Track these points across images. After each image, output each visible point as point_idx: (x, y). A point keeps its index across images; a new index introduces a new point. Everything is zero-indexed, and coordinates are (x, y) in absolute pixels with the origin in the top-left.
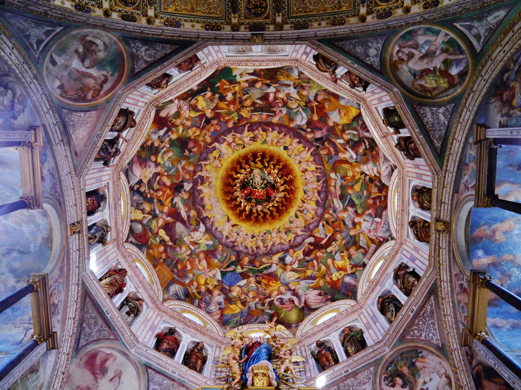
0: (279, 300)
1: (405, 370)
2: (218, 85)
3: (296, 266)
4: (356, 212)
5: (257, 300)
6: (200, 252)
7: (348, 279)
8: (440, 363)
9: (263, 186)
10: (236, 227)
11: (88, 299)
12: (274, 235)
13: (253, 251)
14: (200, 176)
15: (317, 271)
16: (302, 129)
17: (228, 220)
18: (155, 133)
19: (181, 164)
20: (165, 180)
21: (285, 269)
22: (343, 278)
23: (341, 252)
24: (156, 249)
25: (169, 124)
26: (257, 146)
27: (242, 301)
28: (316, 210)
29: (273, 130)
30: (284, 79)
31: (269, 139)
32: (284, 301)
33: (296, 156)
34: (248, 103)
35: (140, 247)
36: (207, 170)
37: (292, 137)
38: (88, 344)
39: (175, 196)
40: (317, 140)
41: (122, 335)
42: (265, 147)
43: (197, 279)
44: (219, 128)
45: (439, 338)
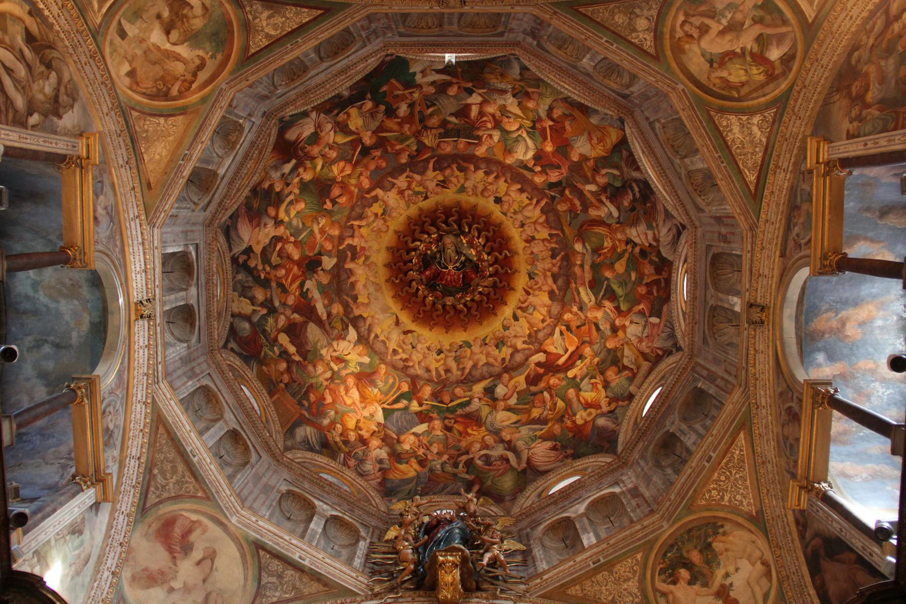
0: (484, 458)
1: (695, 557)
2: (385, 88)
3: (513, 401)
4: (617, 308)
5: (445, 457)
6: (347, 375)
7: (601, 422)
8: (754, 542)
9: (458, 265)
10: (410, 335)
11: (161, 430)
12: (476, 349)
13: (438, 375)
14: (348, 244)
15: (550, 410)
16: (526, 167)
17: (397, 323)
18: (276, 168)
19: (319, 223)
20: (290, 249)
21: (494, 408)
22: (594, 420)
23: (591, 378)
24: (273, 366)
25: (300, 153)
26: (449, 196)
27: (420, 458)
28: (549, 307)
29: (477, 168)
30: (495, 81)
31: (469, 184)
32: (492, 459)
33: (515, 213)
34: (434, 121)
35: (246, 359)
36: (362, 236)
37: (509, 180)
38: (160, 502)
39: (306, 279)
40: (551, 186)
42: (462, 197)
43: (342, 420)
44: (384, 164)
45: (752, 501)
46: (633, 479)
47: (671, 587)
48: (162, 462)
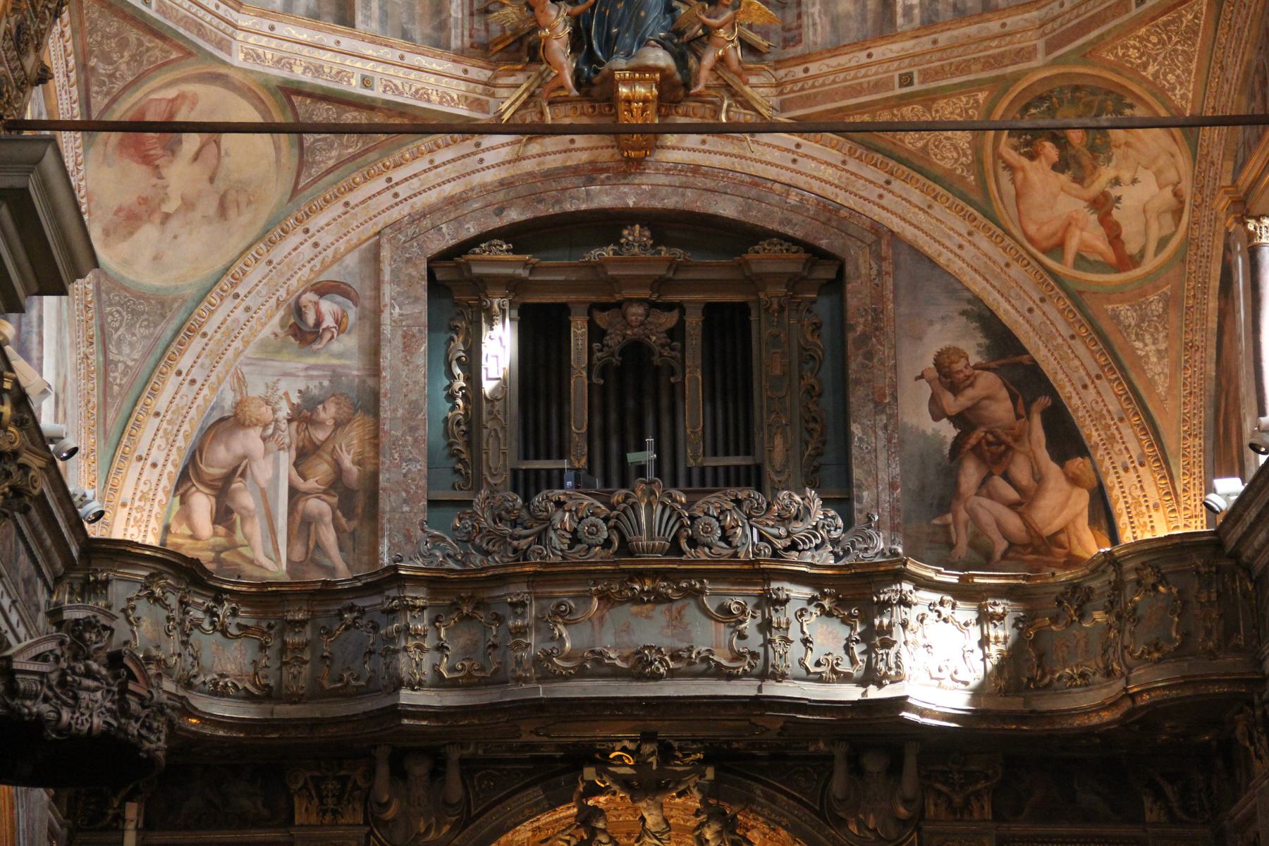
8: (1173, 156)
38: (114, 100)
41: (200, 29)
45: (1190, 95)
47: (1025, 162)
48: (100, 44)
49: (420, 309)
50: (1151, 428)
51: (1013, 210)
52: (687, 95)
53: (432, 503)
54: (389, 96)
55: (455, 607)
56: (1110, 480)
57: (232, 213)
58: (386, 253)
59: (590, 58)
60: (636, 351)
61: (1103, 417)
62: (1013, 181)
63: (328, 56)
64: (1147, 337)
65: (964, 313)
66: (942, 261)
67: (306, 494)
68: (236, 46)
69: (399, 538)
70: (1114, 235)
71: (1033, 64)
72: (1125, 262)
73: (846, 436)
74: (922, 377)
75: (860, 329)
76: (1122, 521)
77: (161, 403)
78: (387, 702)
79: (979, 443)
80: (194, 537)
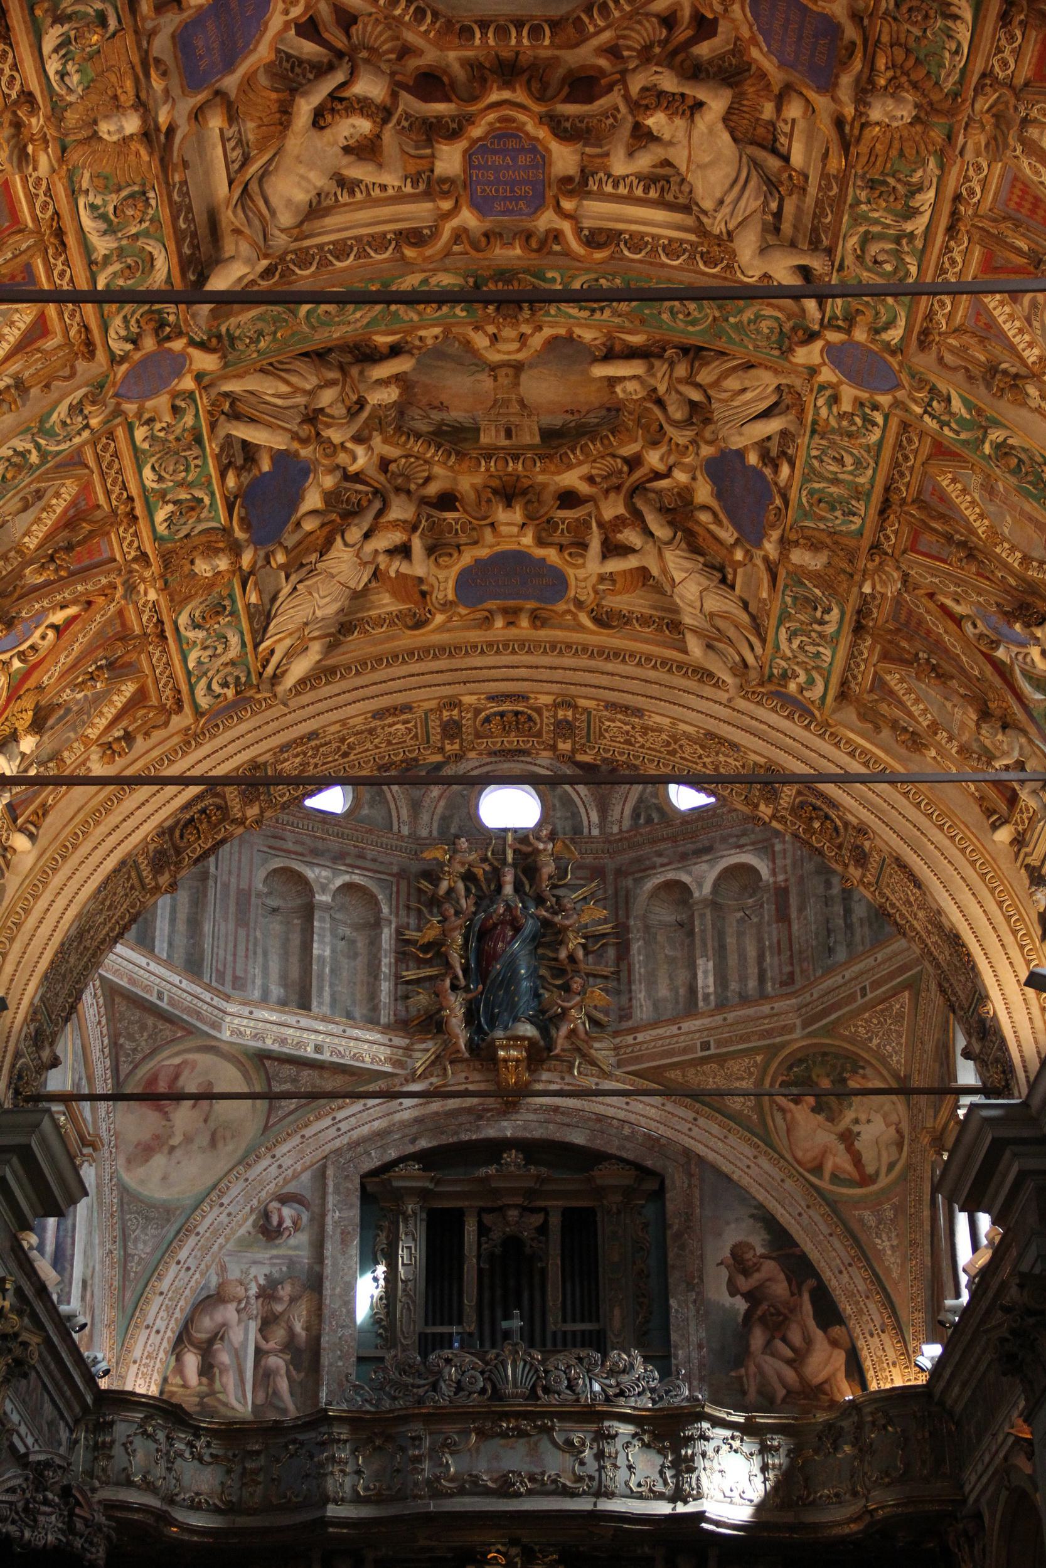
11: (117, 1000)
38: (136, 1067)
41: (198, 1015)
46: (788, 861)
47: (792, 1106)
49: (355, 1213)
50: (889, 1303)
51: (785, 1142)
52: (549, 1058)
53: (361, 1360)
54: (335, 1059)
55: (370, 1440)
56: (861, 1343)
57: (220, 1145)
58: (330, 1172)
59: (479, 1030)
60: (513, 1243)
61: (853, 1295)
62: (785, 1119)
63: (291, 1031)
64: (884, 1236)
65: (752, 1216)
66: (735, 1177)
67: (267, 1352)
68: (225, 1026)
69: (334, 1386)
70: (857, 1160)
71: (794, 1036)
72: (866, 1180)
73: (667, 1308)
74: (721, 1263)
75: (676, 1227)
76: (870, 1374)
77: (165, 1285)
78: (318, 1514)
79: (764, 1315)
80: (185, 1386)
